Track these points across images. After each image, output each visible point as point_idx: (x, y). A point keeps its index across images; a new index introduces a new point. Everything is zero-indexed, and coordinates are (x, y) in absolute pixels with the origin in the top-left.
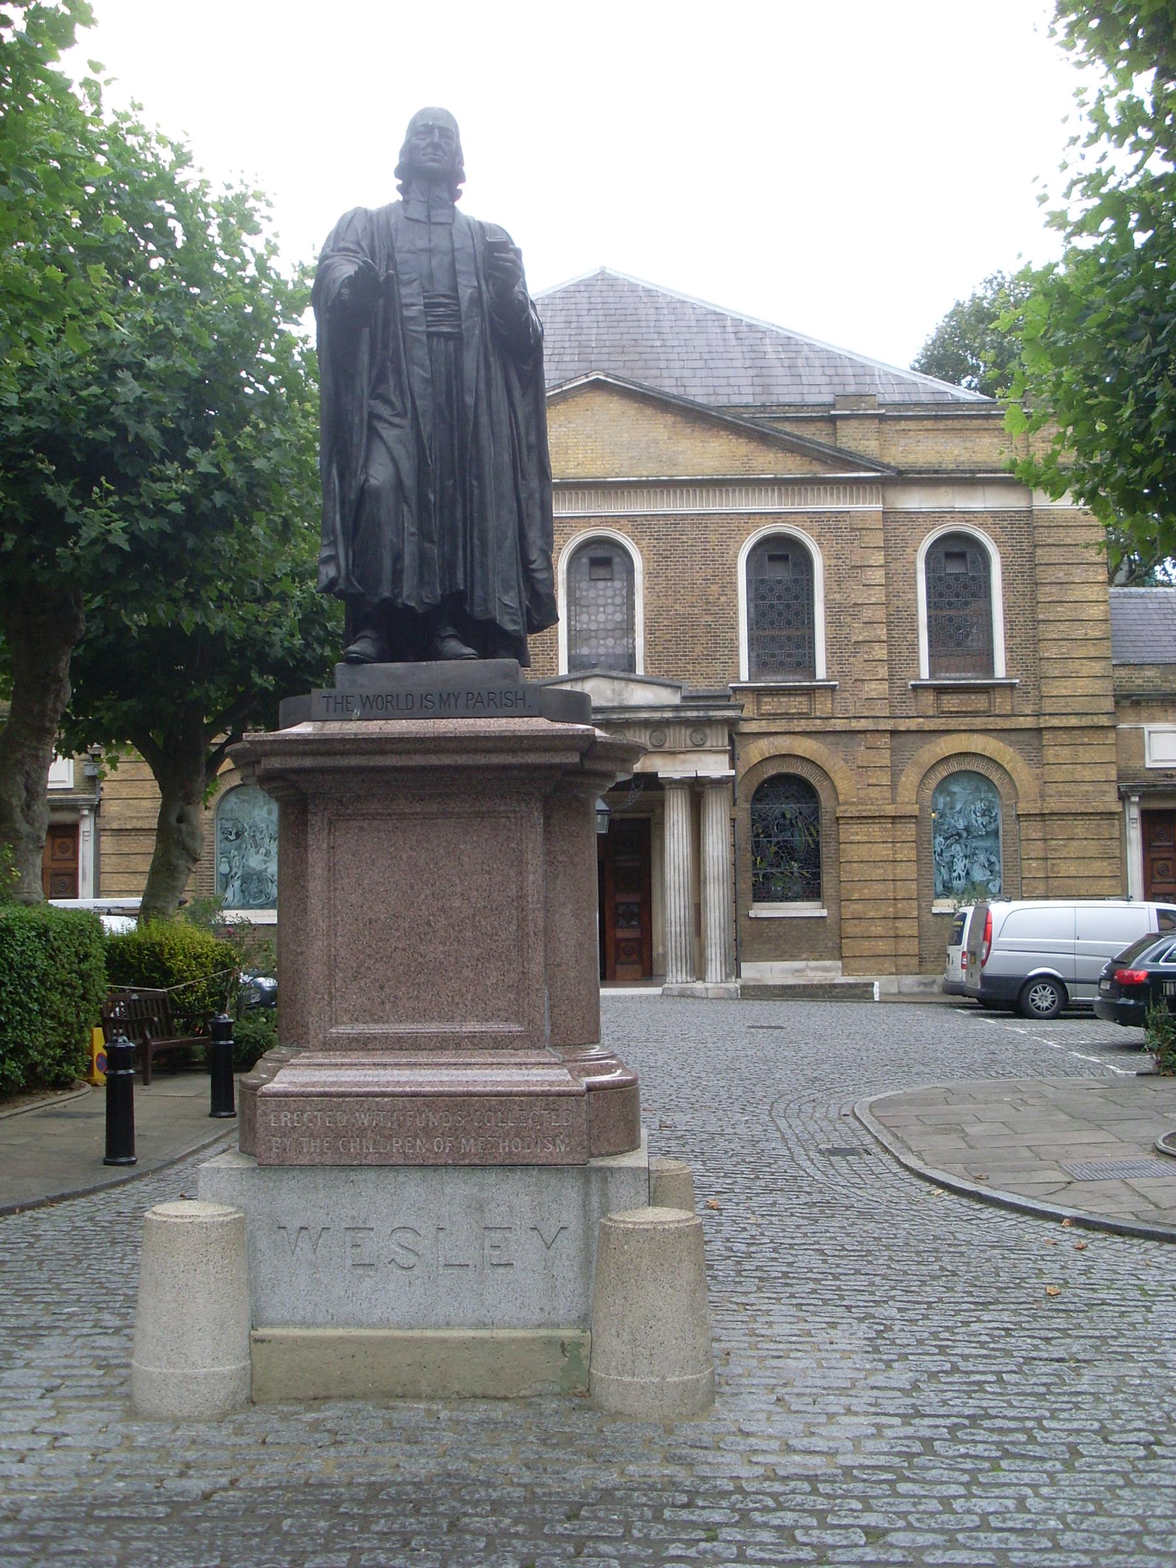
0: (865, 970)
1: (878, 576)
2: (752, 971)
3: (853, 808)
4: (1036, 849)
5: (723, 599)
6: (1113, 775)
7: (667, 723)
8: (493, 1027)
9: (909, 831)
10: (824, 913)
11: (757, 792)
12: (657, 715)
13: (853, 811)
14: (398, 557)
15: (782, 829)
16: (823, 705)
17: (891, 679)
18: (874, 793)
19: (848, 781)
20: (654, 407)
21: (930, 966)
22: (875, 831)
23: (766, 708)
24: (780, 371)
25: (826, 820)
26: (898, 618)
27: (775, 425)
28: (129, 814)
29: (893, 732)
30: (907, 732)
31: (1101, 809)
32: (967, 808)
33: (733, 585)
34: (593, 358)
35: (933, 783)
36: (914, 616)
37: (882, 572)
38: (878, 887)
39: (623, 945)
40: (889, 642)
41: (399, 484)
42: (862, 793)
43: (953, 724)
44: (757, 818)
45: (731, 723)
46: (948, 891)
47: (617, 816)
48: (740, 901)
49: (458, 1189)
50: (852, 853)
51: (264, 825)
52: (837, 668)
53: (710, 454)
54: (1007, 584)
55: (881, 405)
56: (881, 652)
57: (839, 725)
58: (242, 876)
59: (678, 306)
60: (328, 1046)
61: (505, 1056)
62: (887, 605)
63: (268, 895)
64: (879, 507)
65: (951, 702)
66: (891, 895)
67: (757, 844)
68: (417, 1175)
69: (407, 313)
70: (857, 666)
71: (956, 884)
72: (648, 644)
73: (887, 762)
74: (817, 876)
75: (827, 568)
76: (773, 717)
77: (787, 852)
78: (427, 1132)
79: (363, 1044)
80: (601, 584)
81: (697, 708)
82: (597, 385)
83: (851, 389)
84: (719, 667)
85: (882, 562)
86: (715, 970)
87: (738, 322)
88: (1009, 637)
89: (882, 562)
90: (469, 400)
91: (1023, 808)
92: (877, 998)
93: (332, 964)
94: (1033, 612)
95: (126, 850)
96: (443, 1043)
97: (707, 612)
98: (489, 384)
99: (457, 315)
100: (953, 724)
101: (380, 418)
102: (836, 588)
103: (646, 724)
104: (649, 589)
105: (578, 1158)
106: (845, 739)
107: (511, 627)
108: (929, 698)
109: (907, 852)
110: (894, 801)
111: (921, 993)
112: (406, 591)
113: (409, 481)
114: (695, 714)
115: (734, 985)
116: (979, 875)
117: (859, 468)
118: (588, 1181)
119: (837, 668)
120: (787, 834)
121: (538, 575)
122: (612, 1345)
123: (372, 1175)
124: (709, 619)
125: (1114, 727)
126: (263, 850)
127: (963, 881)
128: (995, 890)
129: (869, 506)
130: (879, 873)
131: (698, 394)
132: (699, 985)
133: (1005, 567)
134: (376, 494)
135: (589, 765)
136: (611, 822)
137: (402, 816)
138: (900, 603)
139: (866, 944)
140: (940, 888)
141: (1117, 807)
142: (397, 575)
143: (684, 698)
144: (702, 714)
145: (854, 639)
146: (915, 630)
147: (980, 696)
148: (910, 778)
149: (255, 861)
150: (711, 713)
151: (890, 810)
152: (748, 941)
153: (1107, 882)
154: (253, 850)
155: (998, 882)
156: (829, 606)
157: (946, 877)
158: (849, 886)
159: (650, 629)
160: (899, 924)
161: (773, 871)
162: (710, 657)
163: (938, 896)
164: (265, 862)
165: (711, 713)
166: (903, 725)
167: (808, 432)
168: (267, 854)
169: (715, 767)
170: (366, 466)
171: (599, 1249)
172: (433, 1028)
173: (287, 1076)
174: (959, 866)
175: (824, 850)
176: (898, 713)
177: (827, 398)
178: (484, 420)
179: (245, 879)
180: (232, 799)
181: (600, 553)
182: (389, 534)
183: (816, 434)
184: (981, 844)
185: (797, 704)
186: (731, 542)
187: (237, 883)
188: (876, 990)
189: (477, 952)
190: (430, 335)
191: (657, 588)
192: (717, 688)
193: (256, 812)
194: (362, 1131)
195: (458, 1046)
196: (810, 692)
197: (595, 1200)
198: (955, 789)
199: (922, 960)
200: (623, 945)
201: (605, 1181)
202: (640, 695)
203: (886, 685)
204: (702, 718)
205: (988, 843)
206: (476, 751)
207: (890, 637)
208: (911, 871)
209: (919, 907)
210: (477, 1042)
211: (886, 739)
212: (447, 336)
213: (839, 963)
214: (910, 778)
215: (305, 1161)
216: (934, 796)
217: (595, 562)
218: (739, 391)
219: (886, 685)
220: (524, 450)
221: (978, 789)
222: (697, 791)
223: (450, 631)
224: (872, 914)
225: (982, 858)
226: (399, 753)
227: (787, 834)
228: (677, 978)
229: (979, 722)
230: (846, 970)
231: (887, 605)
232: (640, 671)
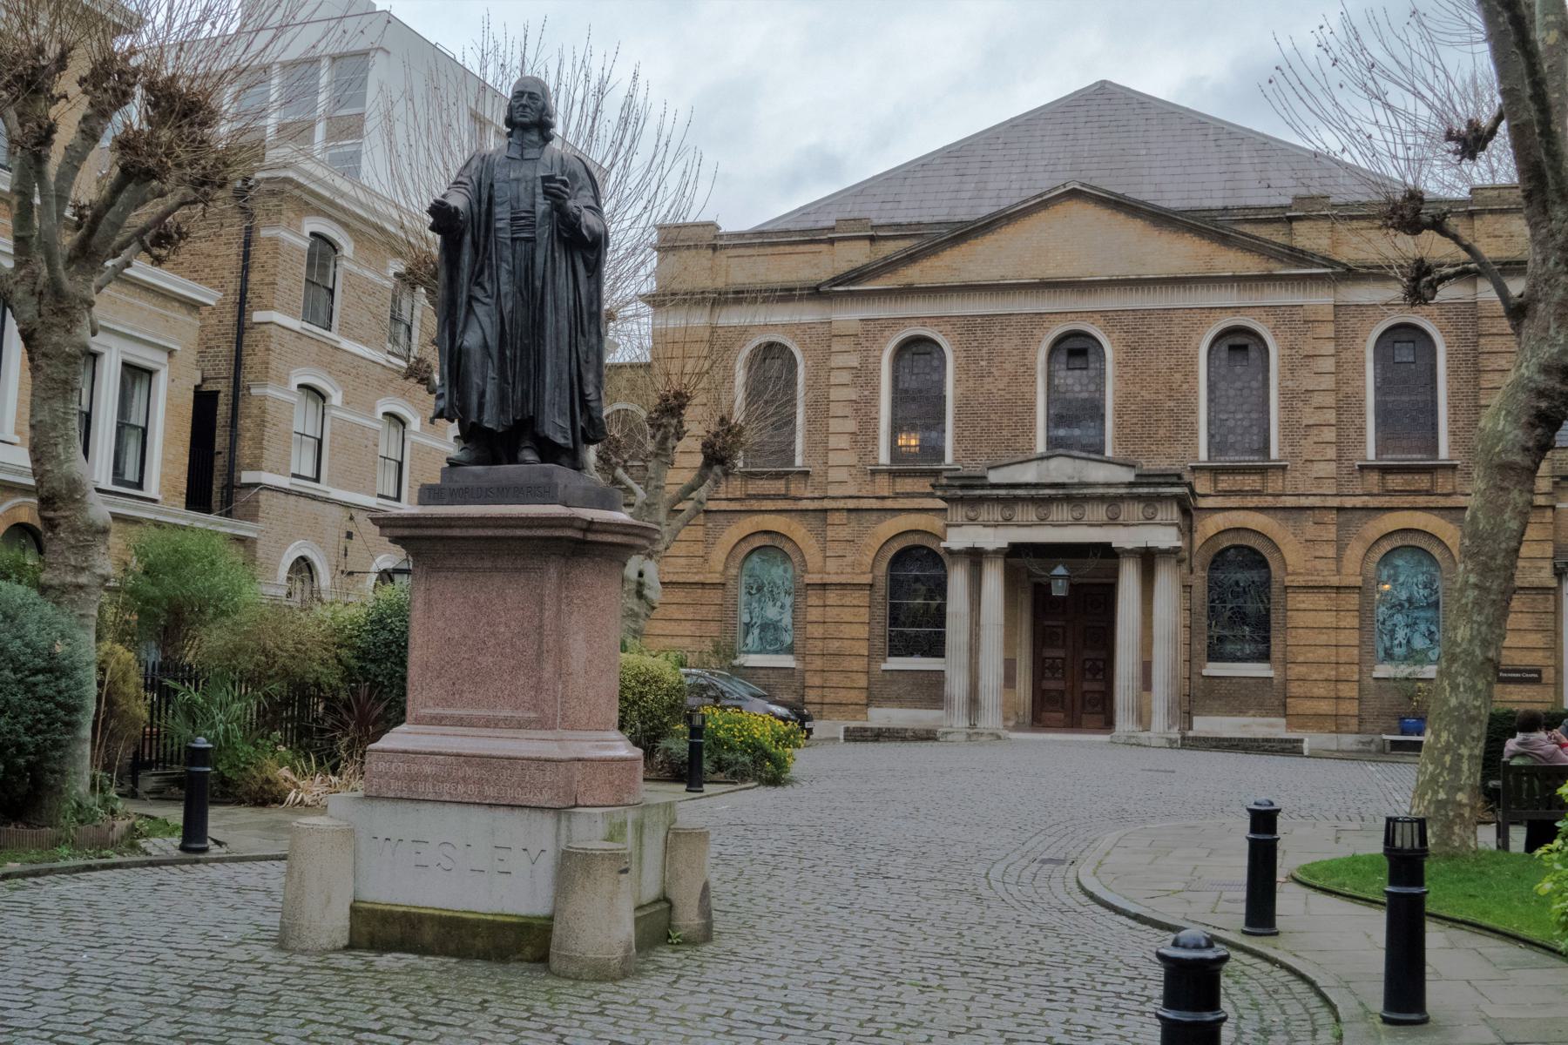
0: (1302, 727)
1: (1328, 365)
2: (1204, 725)
3: (1301, 578)
5: (1185, 386)
6: (1550, 553)
7: (1121, 498)
8: (519, 714)
9: (1354, 600)
10: (1271, 674)
11: (1213, 562)
12: (1112, 491)
13: (1300, 580)
14: (482, 395)
15: (1236, 595)
16: (1275, 483)
17: (1339, 459)
18: (1320, 564)
19: (1297, 553)
20: (1127, 213)
21: (1369, 727)
22: (1320, 600)
23: (1222, 486)
25: (1275, 588)
26: (1347, 405)
27: (1236, 227)
29: (1340, 509)
30: (1354, 509)
31: (1537, 583)
32: (1408, 581)
33: (1195, 373)
34: (1083, 167)
35: (1377, 555)
36: (1361, 403)
37: (1333, 360)
38: (1323, 651)
39: (1088, 696)
40: (1339, 425)
41: (485, 346)
42: (1309, 565)
43: (1396, 501)
44: (1213, 585)
46: (1389, 656)
47: (1077, 580)
48: (1195, 660)
50: (1298, 619)
52: (1289, 449)
54: (1453, 372)
55: (1334, 206)
56: (1330, 435)
57: (1290, 502)
60: (418, 721)
61: (523, 733)
62: (1337, 391)
63: (782, 642)
64: (1331, 301)
65: (1395, 482)
66: (1333, 659)
67: (1212, 609)
68: (455, 808)
69: (499, 225)
70: (1307, 447)
71: (1397, 651)
72: (1119, 426)
73: (1333, 536)
74: (1267, 640)
75: (1282, 357)
78: (464, 779)
79: (438, 720)
80: (1077, 372)
81: (1149, 485)
82: (1074, 194)
83: (1314, 192)
84: (1180, 448)
85: (1332, 351)
86: (1159, 721)
88: (1453, 421)
89: (1332, 351)
90: (538, 284)
92: (1306, 752)
93: (426, 667)
94: (1476, 398)
96: (489, 723)
97: (1170, 398)
98: (554, 273)
99: (533, 225)
100: (1396, 501)
101: (478, 300)
102: (1289, 376)
103: (1102, 499)
104: (1119, 377)
105: (557, 804)
106: (1295, 514)
107: (560, 440)
108: (1374, 477)
109: (1351, 621)
110: (1339, 572)
111: (1359, 751)
112: (486, 418)
113: (493, 343)
114: (1146, 490)
116: (1419, 643)
117: (1312, 264)
118: (559, 820)
119: (1289, 449)
120: (1239, 602)
121: (593, 404)
123: (429, 805)
124: (1172, 404)
125: (1553, 508)
127: (1404, 649)
128: (1434, 658)
129: (1320, 300)
130: (1323, 639)
131: (1172, 200)
132: (1146, 734)
133: (1450, 355)
134: (468, 350)
135: (591, 537)
136: (1073, 588)
137: (471, 570)
138: (1349, 390)
139: (1309, 703)
140: (1382, 654)
141: (1553, 583)
142: (481, 406)
143: (1137, 476)
144: (1152, 490)
145: (1305, 422)
146: (1362, 415)
147: (1423, 477)
148: (1355, 551)
149: (772, 612)
150: (1161, 490)
151: (1334, 581)
153: (1541, 654)
155: (1437, 651)
156: (1283, 394)
157: (1388, 644)
158: (1294, 649)
159: (1119, 414)
160: (1341, 686)
161: (1225, 633)
162: (1172, 439)
163: (1382, 662)
165: (1161, 490)
166: (1349, 502)
167: (1264, 232)
168: (782, 607)
169: (1164, 537)
170: (464, 331)
172: (483, 712)
173: (394, 739)
174: (1401, 635)
175: (1273, 616)
176: (1345, 491)
177: (1287, 201)
178: (549, 298)
179: (764, 628)
180: (755, 558)
181: (1077, 344)
182: (476, 379)
184: (1422, 614)
185: (1252, 482)
186: (1193, 334)
187: (756, 631)
188: (1306, 746)
189: (513, 662)
190: (513, 240)
191: (1126, 376)
192: (1177, 467)
193: (773, 571)
194: (426, 777)
195: (496, 726)
196: (1262, 471)
197: (563, 832)
198: (1400, 562)
199: (1361, 721)
200: (1088, 696)
201: (569, 820)
202: (1098, 473)
203: (1333, 465)
205: (1429, 614)
206: (551, 527)
207: (1339, 421)
208: (1353, 638)
209: (1361, 672)
210: (508, 723)
211: (1333, 515)
212: (527, 240)
213: (1283, 721)
214: (1355, 551)
215: (392, 795)
216: (1378, 569)
217: (1074, 353)
218: (1210, 194)
219: (1333, 465)
220: (585, 317)
221: (1420, 563)
222: (1148, 559)
223: (528, 444)
224: (1315, 676)
225: (1423, 627)
226: (460, 527)
227: (1239, 602)
228: (1124, 723)
229: (1421, 501)
230: (1289, 726)
231: (1337, 391)
232: (1109, 453)
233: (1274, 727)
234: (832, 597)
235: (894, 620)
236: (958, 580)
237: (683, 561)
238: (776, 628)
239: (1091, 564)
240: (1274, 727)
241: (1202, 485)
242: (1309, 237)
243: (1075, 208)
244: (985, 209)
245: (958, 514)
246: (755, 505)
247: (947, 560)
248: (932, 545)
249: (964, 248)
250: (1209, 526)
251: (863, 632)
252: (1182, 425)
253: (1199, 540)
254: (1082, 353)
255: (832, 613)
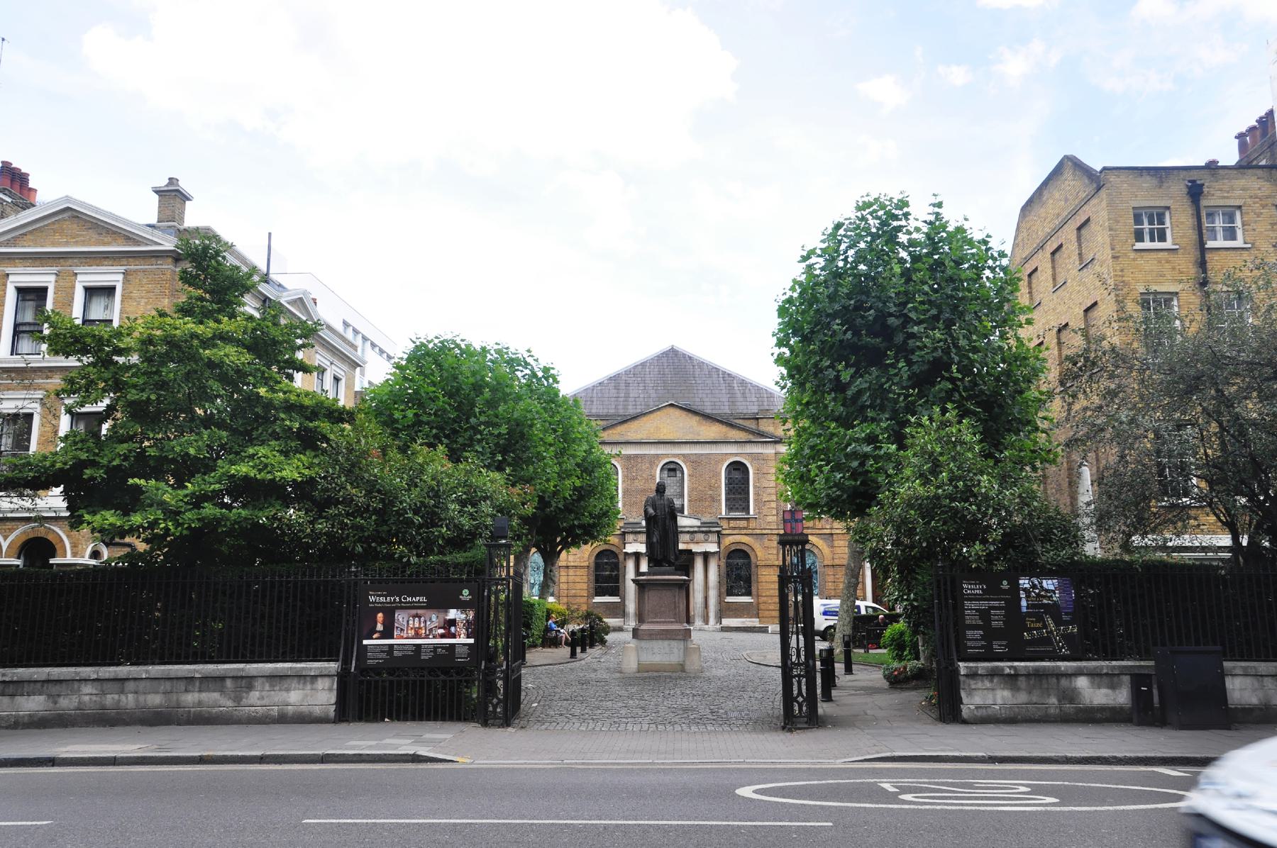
2: (727, 622)
4: (831, 578)
16: (752, 524)
24: (739, 395)
44: (728, 565)
45: (718, 532)
49: (666, 643)
50: (762, 579)
53: (713, 431)
57: (758, 532)
59: (701, 364)
76: (735, 528)
77: (739, 578)
82: (672, 405)
86: (712, 620)
87: (724, 373)
91: (826, 563)
115: (718, 626)
122: (688, 663)
129: (769, 450)
152: (725, 611)
156: (755, 487)
167: (748, 424)
169: (712, 548)
171: (686, 649)
181: (672, 466)
183: (751, 425)
185: (743, 524)
204: (708, 530)
217: (670, 470)
222: (706, 556)
233: (754, 622)
234: (571, 572)
235: (597, 581)
236: (630, 565)
239: (684, 557)
240: (754, 622)
241: (724, 524)
242: (766, 426)
243: (671, 410)
244: (631, 411)
245: (630, 538)
247: (621, 557)
248: (614, 549)
249: (626, 425)
250: (727, 541)
251: (585, 586)
252: (715, 499)
253: (722, 547)
254: (674, 470)
255: (571, 579)
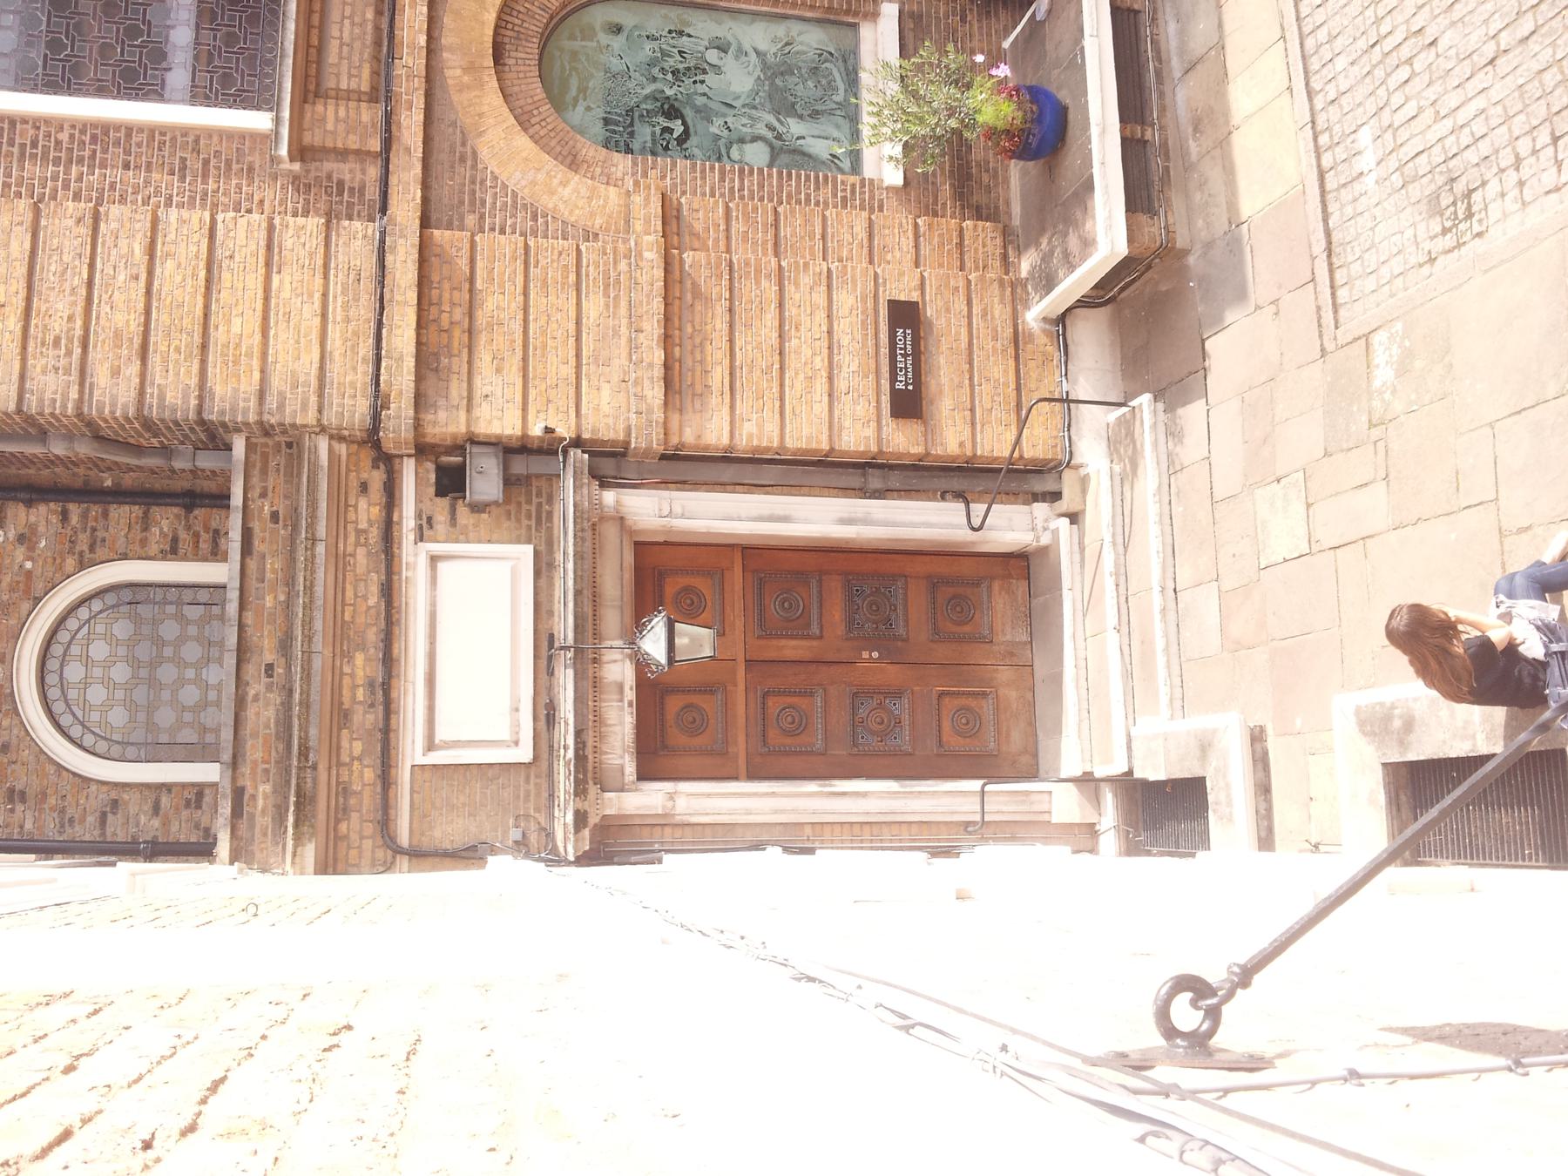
28: (620, 361)
51: (649, 46)
58: (777, 112)
63: (824, 55)
95: (718, 376)
126: (712, 56)
149: (738, 79)
154: (711, 79)
164: (741, 52)
168: (723, 49)
179: (785, 106)
187: (795, 127)
237: (593, 307)
238: (786, 70)
246: (411, 60)
